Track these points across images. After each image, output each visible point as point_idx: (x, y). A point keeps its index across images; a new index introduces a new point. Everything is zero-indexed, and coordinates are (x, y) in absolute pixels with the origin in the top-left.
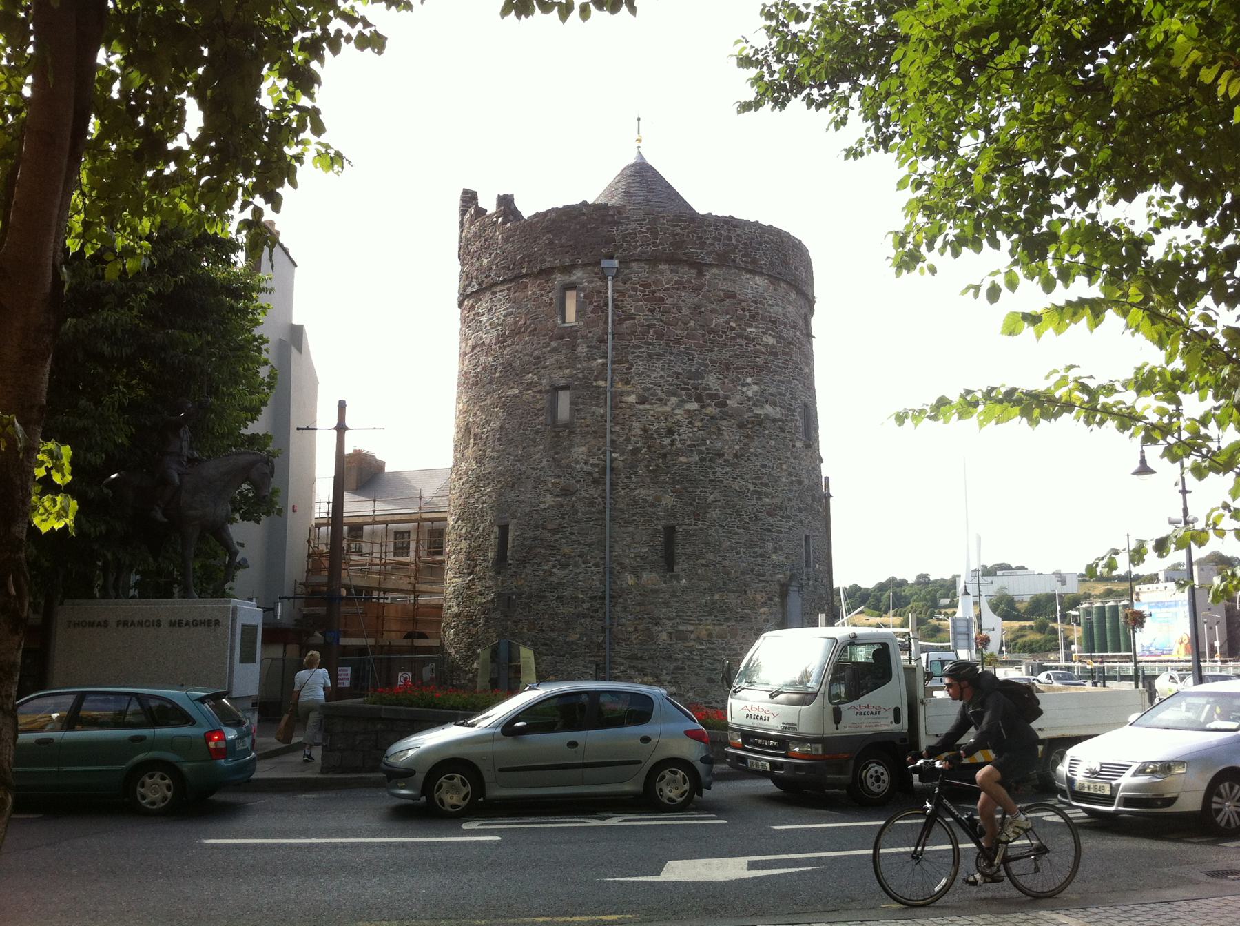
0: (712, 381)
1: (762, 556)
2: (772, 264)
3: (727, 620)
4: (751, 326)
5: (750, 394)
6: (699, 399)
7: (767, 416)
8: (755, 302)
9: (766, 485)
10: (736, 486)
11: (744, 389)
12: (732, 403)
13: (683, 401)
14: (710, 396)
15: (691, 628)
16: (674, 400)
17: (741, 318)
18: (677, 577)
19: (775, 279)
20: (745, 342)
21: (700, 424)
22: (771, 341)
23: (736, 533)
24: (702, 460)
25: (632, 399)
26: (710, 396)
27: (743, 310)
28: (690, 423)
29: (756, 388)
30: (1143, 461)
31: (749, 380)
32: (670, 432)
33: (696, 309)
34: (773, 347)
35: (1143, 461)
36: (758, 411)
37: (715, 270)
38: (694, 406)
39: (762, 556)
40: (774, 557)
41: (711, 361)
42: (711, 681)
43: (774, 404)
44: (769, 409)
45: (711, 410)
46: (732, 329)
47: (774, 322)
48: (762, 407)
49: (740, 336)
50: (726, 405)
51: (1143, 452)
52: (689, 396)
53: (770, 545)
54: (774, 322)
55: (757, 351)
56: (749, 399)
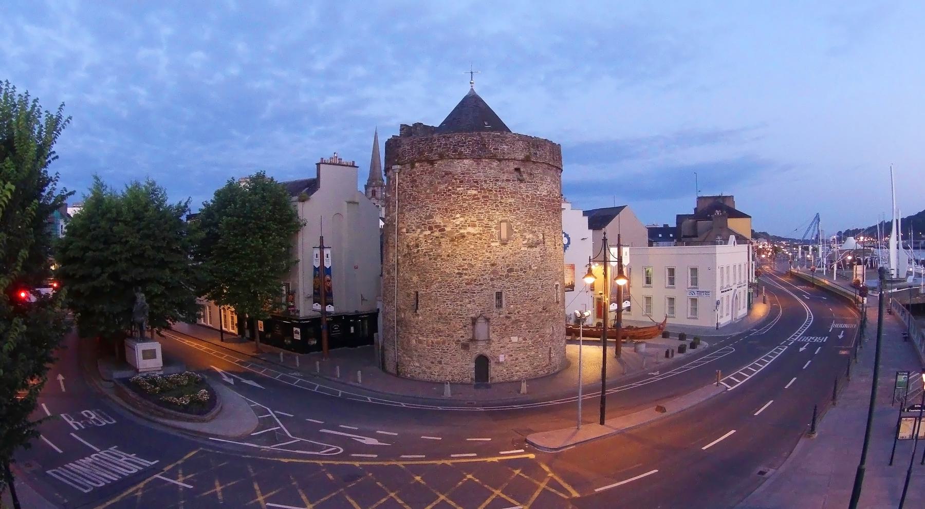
0: (438, 220)
2: (473, 151)
6: (430, 228)
7: (468, 233)
9: (466, 269)
10: (448, 271)
12: (448, 229)
13: (422, 231)
14: (436, 227)
16: (419, 230)
18: (418, 315)
19: (478, 159)
22: (474, 192)
25: (404, 230)
26: (436, 227)
29: (462, 219)
31: (458, 216)
32: (417, 246)
33: (431, 184)
34: (475, 195)
36: (462, 231)
37: (440, 162)
38: (428, 232)
40: (469, 306)
42: (432, 363)
43: (474, 226)
44: (470, 230)
45: (437, 234)
47: (477, 182)
49: (454, 193)
50: (444, 230)
53: (467, 300)
54: (477, 182)
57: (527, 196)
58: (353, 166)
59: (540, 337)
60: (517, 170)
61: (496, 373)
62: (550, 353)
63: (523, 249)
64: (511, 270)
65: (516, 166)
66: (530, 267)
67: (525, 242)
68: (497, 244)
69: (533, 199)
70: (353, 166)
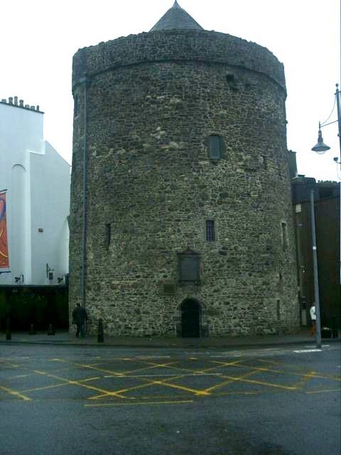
0: (135, 135)
1: (163, 236)
3: (138, 277)
4: (160, 95)
5: (159, 137)
7: (172, 149)
8: (163, 79)
11: (154, 135)
15: (118, 282)
16: (112, 149)
17: (152, 92)
20: (155, 106)
21: (126, 161)
22: (178, 101)
23: (146, 225)
24: (125, 183)
27: (155, 86)
28: (120, 162)
29: (162, 132)
30: (320, 139)
34: (178, 103)
35: (320, 139)
39: (163, 236)
41: (134, 122)
43: (178, 141)
45: (134, 152)
46: (149, 99)
48: (167, 144)
49: (153, 103)
51: (320, 132)
52: (120, 146)
55: (166, 109)
56: (158, 140)
57: (243, 110)
58: (38, 111)
59: (264, 283)
60: (230, 78)
61: (211, 323)
62: (278, 307)
63: (238, 170)
64: (224, 196)
65: (228, 72)
66: (249, 195)
67: (241, 163)
68: (206, 162)
69: (250, 114)
70: (38, 111)
